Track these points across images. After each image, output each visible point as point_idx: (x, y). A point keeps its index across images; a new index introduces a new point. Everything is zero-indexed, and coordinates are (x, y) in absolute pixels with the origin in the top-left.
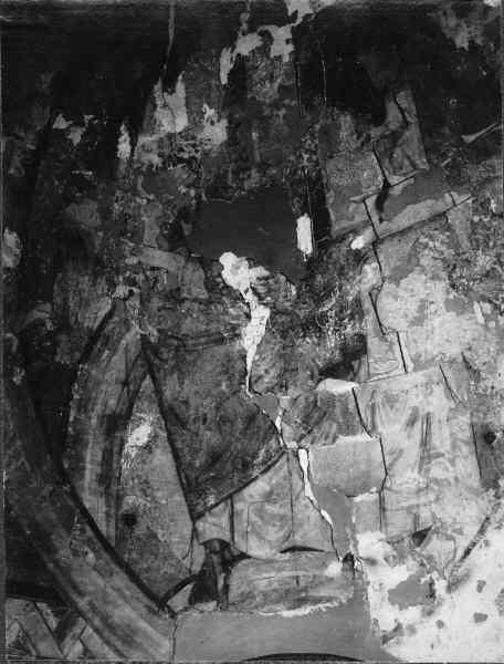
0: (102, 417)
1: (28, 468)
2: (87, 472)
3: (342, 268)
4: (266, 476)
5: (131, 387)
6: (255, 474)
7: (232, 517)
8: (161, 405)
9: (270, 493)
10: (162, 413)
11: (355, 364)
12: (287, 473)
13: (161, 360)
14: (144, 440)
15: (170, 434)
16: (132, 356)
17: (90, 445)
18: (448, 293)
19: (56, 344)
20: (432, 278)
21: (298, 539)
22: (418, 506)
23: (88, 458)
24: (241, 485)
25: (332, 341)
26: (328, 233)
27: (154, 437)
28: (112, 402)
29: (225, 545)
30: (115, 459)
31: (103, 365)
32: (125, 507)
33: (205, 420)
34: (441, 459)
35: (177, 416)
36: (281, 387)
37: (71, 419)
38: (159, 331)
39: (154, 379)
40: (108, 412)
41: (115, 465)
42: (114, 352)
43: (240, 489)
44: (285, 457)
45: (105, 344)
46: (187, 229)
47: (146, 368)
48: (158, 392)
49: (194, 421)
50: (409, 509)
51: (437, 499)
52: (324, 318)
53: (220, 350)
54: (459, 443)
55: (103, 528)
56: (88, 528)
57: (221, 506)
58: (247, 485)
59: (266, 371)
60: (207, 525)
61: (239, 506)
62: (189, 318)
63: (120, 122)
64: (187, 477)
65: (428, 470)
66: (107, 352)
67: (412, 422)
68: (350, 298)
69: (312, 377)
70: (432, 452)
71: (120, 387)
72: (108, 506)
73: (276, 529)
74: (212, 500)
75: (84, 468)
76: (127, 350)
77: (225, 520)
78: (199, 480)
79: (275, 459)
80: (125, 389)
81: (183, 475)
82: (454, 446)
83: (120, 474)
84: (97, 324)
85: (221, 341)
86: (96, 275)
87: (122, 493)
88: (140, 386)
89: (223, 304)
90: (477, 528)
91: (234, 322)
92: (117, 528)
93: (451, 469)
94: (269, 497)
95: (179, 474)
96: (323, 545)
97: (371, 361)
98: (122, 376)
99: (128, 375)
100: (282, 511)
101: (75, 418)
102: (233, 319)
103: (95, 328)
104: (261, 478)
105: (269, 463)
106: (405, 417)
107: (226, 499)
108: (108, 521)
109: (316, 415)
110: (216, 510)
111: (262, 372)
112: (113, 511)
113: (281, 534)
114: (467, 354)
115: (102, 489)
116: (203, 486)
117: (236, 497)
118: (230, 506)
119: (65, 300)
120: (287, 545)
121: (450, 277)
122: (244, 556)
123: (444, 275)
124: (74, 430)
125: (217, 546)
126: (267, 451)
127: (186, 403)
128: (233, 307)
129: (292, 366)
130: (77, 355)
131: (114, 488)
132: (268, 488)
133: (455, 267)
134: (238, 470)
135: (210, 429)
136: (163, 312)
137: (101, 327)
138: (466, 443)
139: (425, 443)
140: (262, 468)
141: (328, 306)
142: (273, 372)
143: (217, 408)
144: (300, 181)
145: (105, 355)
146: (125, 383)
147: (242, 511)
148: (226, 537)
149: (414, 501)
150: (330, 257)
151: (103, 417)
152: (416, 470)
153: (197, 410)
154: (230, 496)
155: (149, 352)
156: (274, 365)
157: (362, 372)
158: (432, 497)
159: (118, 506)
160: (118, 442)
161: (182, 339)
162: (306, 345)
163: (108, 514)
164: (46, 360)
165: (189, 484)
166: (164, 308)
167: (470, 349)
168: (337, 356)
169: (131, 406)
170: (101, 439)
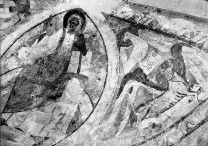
3: (65, 79)
4: (24, 112)
5: (10, 83)
6: (22, 110)
7: (11, 116)
8: (13, 89)
9: (23, 115)
10: (12, 90)
11: (57, 98)
12: (28, 113)
13: (19, 81)
14: (4, 94)
15: (11, 95)
16: (14, 78)
18: (83, 91)
20: (81, 87)
21: (20, 127)
22: (50, 132)
24: (17, 111)
25: (55, 92)
26: (66, 72)
27: (7, 94)
29: (4, 121)
31: (7, 77)
33: (20, 96)
34: (61, 124)
35: (15, 92)
36: (39, 96)
38: (22, 76)
39: (15, 83)
43: (17, 112)
44: (31, 110)
46: (40, 61)
48: (14, 86)
49: (18, 95)
50: (48, 132)
51: (55, 132)
52: (56, 87)
53: (32, 85)
54: (67, 122)
57: (10, 113)
58: (19, 112)
59: (38, 92)
60: (4, 115)
61: (13, 115)
62: (30, 76)
63: (37, 38)
64: (8, 105)
65: (58, 125)
67: (61, 114)
68: (63, 85)
69: (46, 97)
70: (61, 122)
71: (7, 82)
73: (17, 123)
74: (9, 111)
76: (14, 76)
77: (8, 116)
78: (10, 106)
79: (28, 109)
80: (8, 83)
81: (7, 104)
82: (66, 122)
84: (11, 69)
85: (34, 83)
86: (17, 61)
89: (38, 76)
90: (59, 141)
91: (39, 81)
93: (62, 127)
94: (21, 116)
95: (7, 103)
96: (24, 131)
97: (61, 99)
98: (9, 80)
100: (22, 120)
102: (39, 80)
104: (23, 112)
105: (27, 110)
106: (60, 113)
107: (12, 112)
109: (43, 105)
110: (8, 113)
111: (37, 92)
113: (18, 124)
114: (80, 104)
116: (10, 108)
117: (14, 113)
118: (12, 114)
119: (8, 63)
120: (17, 127)
121: (85, 88)
122: (6, 125)
123: (84, 87)
125: (3, 120)
126: (28, 107)
127: (18, 91)
128: (40, 78)
129: (44, 93)
132: (22, 114)
133: (86, 87)
134: (19, 108)
135: (19, 98)
136: (26, 73)
137: (11, 70)
138: (69, 122)
139: (61, 119)
140: (24, 110)
141: (59, 85)
142: (40, 93)
143: (24, 95)
144: (65, 61)
145: (8, 75)
146: (9, 82)
147: (14, 116)
148: (6, 119)
149: (50, 131)
150: (64, 76)
152: (55, 124)
153: (20, 93)
154: (14, 112)
155: (18, 79)
156: (41, 92)
157: (57, 100)
158: (54, 131)
161: (26, 79)
162: (49, 91)
165: (7, 106)
166: (26, 72)
167: (80, 104)
168: (55, 95)
169: (8, 86)
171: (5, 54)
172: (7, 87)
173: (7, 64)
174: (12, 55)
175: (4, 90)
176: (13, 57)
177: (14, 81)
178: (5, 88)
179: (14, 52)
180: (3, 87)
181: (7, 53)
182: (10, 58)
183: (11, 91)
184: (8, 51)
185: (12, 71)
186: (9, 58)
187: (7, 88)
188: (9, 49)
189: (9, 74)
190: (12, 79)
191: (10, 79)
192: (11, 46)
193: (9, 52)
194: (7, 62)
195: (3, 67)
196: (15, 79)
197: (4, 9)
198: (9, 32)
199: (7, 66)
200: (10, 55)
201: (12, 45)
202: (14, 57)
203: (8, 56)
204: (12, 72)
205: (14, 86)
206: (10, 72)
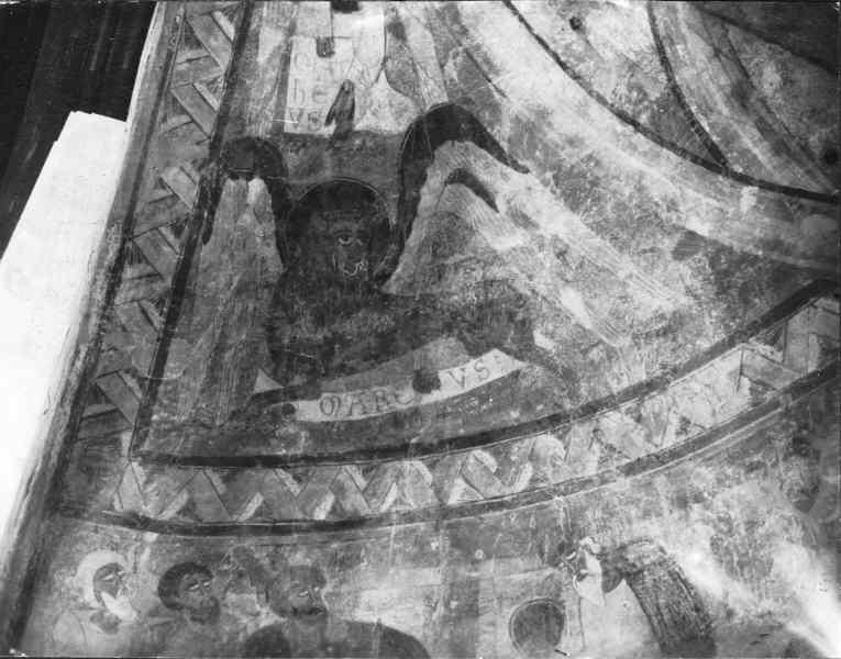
0: (728, 99)
1: (714, 203)
2: (760, 157)
5: (725, 50)
8: (760, 35)
10: (767, 40)
14: (777, 78)
17: (740, 132)
19: (640, 89)
23: (750, 145)
27: (783, 67)
28: (723, 80)
30: (770, 121)
32: (817, 152)
37: (707, 129)
39: (732, 22)
40: (728, 90)
41: (776, 127)
42: (684, 40)
45: (672, 43)
47: (718, 20)
55: (814, 187)
56: (804, 201)
66: (678, 47)
71: (716, 62)
72: (800, 163)
75: (755, 157)
76: (690, 26)
80: (723, 58)
83: (786, 129)
87: (803, 143)
88: (729, 41)
92: (826, 175)
98: (709, 49)
99: (712, 45)
101: (709, 125)
103: (653, 42)
108: (814, 177)
112: (810, 166)
115: (785, 157)
124: (718, 136)
130: (663, 77)
131: (793, 145)
137: (656, 36)
145: (681, 53)
146: (717, 53)
151: (728, 98)
159: (811, 157)
160: (759, 104)
163: (809, 172)
164: (647, 108)
169: (738, 62)
170: (743, 118)
171: (563, 59)
172: (744, 64)
173: (619, 55)
174: (576, 25)
175: (755, 80)
176: (589, 22)
177: (717, 30)
178: (747, 75)
179: (563, 17)
180: (740, 83)
181: (559, 52)
182: (591, 38)
183: (768, 45)
184: (552, 46)
185: (662, 33)
186: (588, 42)
187: (751, 67)
188: (545, 38)
189: (675, 52)
190: (706, 35)
191: (702, 44)
192: (528, 27)
193: (558, 37)
194: (609, 55)
195: (632, 75)
196: (709, 23)
197: (339, 37)
198: (456, 28)
199: (632, 57)
200: (571, 36)
201: (522, 19)
202: (587, 19)
203: (578, 48)
204: (669, 37)
205: (747, 28)
206: (666, 43)
